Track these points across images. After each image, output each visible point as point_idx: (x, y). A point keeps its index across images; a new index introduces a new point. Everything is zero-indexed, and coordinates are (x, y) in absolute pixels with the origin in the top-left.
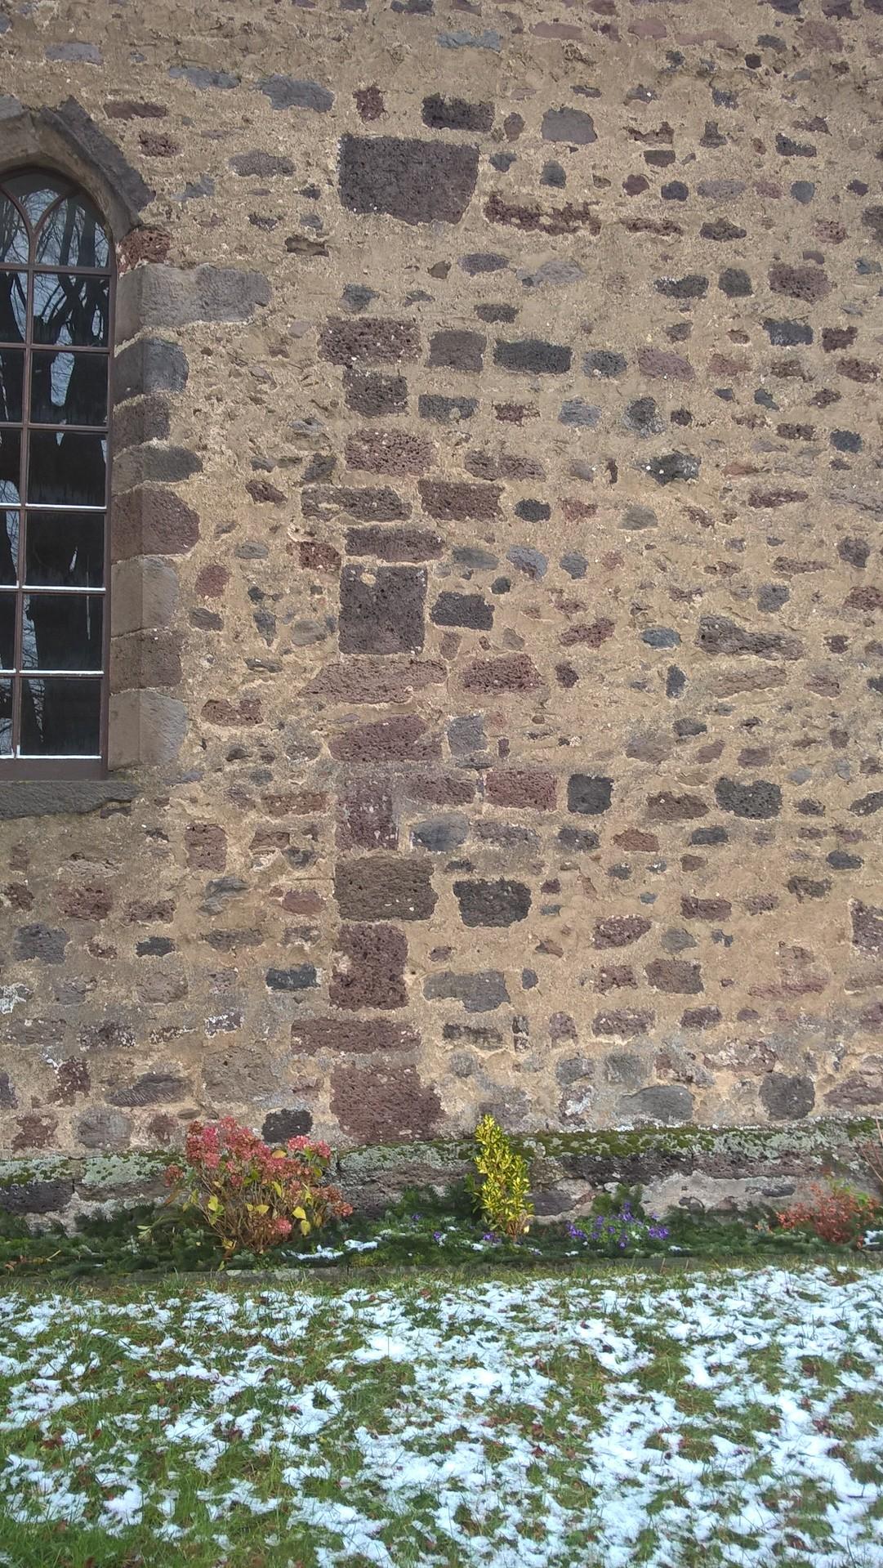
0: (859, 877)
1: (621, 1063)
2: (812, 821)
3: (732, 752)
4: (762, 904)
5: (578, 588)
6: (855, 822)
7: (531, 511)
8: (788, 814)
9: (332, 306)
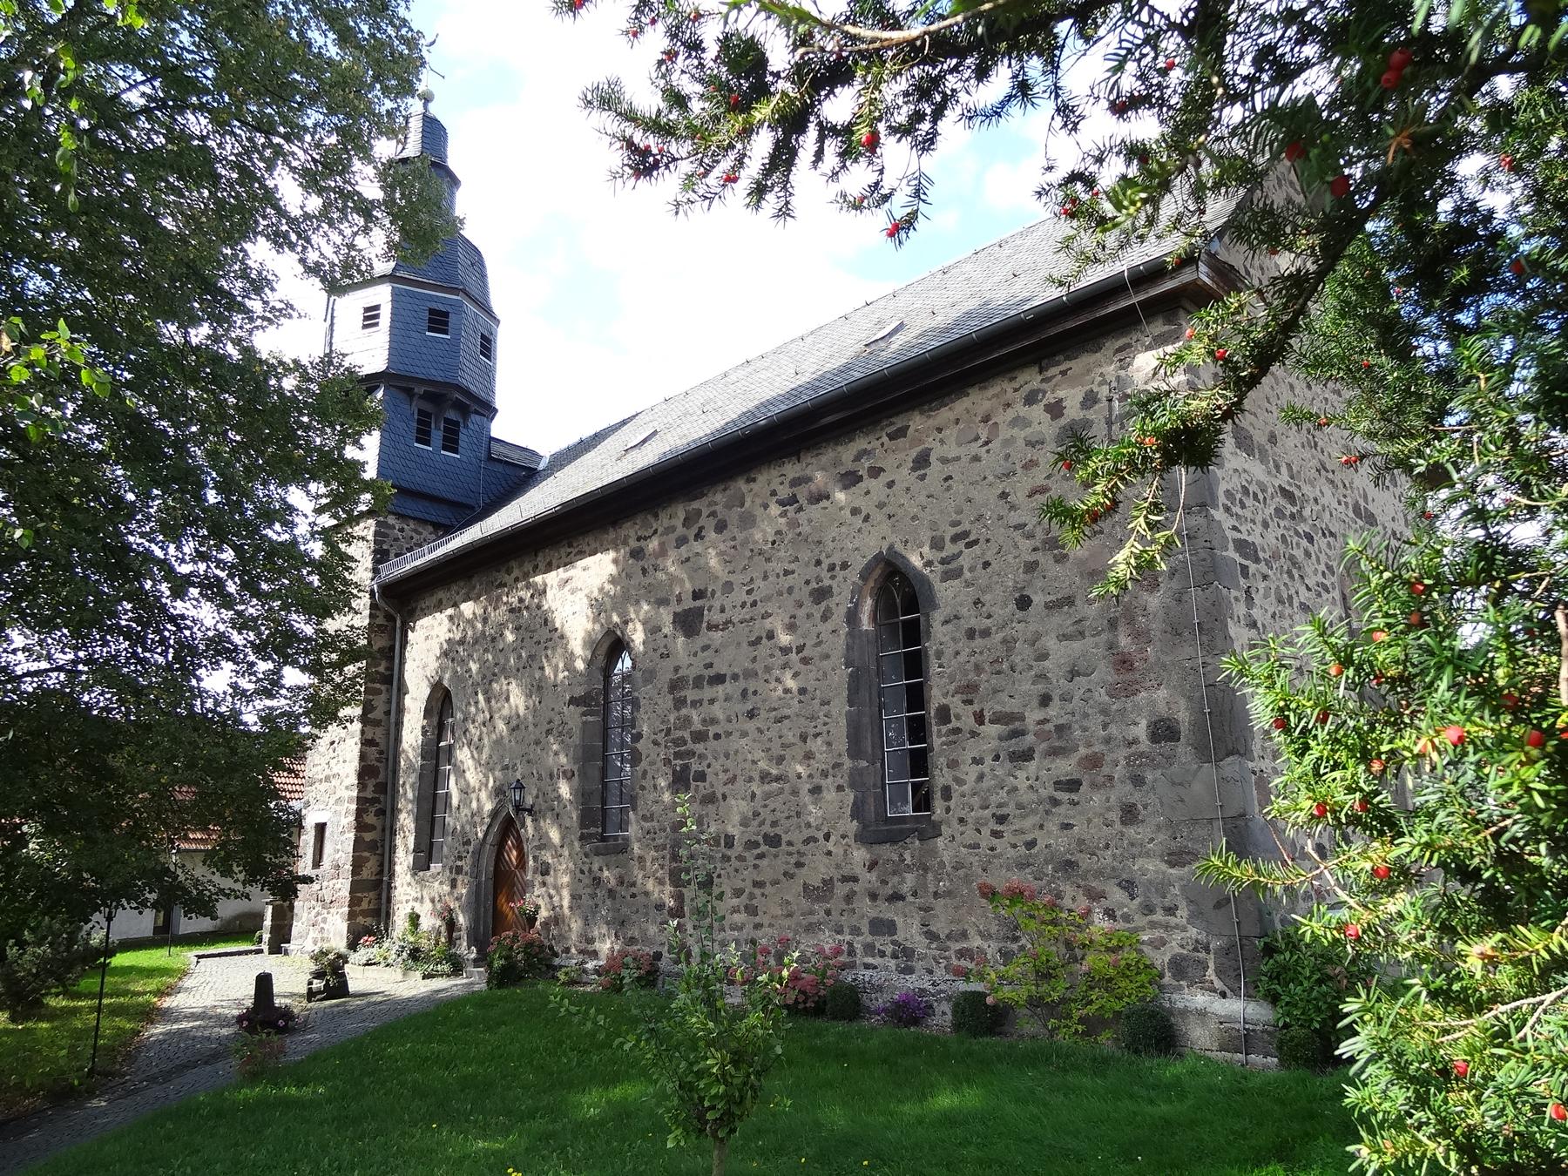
0: (804, 871)
3: (768, 822)
4: (775, 883)
5: (729, 764)
6: (803, 848)
7: (717, 736)
8: (784, 846)
9: (670, 675)
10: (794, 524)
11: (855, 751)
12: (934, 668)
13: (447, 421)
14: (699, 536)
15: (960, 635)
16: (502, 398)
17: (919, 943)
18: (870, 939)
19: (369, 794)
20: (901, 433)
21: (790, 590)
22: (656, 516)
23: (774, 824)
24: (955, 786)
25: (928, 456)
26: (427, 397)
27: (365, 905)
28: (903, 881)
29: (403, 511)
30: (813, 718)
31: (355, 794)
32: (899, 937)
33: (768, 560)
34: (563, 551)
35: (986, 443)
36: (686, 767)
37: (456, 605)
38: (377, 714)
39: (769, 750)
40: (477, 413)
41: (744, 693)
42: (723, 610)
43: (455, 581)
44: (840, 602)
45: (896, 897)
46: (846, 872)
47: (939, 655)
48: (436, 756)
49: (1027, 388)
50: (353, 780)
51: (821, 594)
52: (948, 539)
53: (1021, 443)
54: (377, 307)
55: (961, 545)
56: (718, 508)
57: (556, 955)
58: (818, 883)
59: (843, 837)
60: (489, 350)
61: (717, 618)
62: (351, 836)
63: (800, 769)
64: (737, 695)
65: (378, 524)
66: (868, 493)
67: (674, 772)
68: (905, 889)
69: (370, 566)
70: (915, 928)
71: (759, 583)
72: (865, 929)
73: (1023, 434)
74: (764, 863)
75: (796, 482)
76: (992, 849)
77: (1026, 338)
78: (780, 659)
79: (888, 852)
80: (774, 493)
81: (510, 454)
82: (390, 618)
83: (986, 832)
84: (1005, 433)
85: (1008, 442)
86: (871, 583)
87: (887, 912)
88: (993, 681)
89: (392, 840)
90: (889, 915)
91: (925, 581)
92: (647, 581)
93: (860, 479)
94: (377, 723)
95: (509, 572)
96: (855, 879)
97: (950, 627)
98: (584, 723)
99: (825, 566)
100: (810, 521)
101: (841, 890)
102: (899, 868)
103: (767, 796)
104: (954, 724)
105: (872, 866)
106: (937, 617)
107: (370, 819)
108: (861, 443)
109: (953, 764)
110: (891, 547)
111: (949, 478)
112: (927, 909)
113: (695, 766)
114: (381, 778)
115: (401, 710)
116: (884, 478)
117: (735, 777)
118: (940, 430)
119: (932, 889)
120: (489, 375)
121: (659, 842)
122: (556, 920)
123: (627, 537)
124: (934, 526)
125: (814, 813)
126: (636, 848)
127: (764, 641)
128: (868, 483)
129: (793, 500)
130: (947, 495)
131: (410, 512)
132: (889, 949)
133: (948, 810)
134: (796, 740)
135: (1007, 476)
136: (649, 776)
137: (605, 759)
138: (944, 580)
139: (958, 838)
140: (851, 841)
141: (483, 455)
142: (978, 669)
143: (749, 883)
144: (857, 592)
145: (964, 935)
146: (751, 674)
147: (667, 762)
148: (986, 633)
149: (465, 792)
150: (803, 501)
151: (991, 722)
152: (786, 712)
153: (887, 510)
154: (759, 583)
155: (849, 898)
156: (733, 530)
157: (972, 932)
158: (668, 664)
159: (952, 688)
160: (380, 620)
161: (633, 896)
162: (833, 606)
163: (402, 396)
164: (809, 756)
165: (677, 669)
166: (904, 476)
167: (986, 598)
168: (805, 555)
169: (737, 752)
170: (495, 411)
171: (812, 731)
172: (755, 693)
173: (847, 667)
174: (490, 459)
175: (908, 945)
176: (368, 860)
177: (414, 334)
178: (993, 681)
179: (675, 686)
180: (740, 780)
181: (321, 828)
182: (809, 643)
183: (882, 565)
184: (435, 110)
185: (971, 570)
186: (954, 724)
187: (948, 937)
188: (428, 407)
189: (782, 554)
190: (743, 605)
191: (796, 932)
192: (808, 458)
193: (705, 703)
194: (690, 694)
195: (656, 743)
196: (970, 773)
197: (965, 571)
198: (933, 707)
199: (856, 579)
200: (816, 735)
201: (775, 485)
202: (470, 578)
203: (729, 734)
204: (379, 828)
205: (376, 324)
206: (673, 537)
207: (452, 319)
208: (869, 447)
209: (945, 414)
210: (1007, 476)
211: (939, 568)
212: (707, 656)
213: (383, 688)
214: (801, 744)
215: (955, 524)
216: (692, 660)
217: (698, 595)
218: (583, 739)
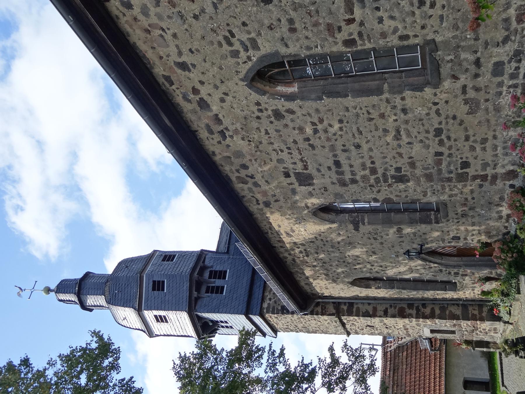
0: (458, 115)
1: (504, 148)
2: (444, 123)
3: (427, 135)
4: (466, 129)
5: (390, 156)
6: (443, 116)
7: (373, 163)
8: (443, 126)
10: (236, 131)
11: (379, 91)
12: (319, 50)
13: (210, 277)
14: (252, 177)
15: (294, 36)
16: (196, 247)
17: (510, 47)
18: (506, 76)
19: (414, 312)
20: (168, 79)
21: (277, 131)
22: (243, 197)
23: (427, 132)
24: (399, 33)
25: (179, 63)
26: (198, 290)
27: (476, 312)
28: (466, 60)
29: (260, 299)
30: (358, 115)
31: (414, 320)
32: (505, 59)
33: (261, 143)
34: (270, 235)
35: (163, 30)
36: (393, 177)
37: (307, 278)
38: (370, 309)
39: (379, 137)
40: (204, 262)
41: (344, 151)
42: (295, 163)
43: (295, 279)
44: (282, 105)
45: (477, 63)
46: (459, 92)
47: (308, 48)
49: (121, 8)
50: (407, 321)
51: (278, 115)
52: (230, 48)
53: (158, 10)
54: (156, 316)
55: (233, 40)
56: (233, 169)
57: (509, 233)
58: (467, 107)
59: (435, 95)
60: (170, 256)
61: (299, 167)
62: (437, 321)
63: (391, 120)
64: (346, 154)
65: (268, 312)
66: (209, 95)
67: (395, 182)
68: (471, 58)
69: (290, 316)
70: (500, 50)
71: (276, 146)
72: (499, 79)
73: (152, 9)
74: (453, 136)
75: (211, 132)
76: (443, 7)
77: (87, 17)
78: (321, 134)
79: (446, 69)
80: (219, 142)
81: (224, 240)
82: (318, 304)
83: (431, 12)
84: (154, 20)
85: (160, 17)
86: (267, 88)
87: (488, 66)
88: (324, 15)
89: (439, 300)
90: (490, 66)
91: (261, 59)
92: (281, 198)
93: (201, 99)
94: (375, 309)
95: (287, 258)
96: (464, 87)
97: (289, 43)
98: (369, 223)
99: (260, 114)
100: (233, 124)
101: (471, 94)
102: (457, 62)
103: (409, 135)
104: (355, 36)
105: (455, 78)
106: (283, 51)
107: (428, 311)
108: (179, 99)
109: (384, 35)
110: (242, 80)
111: (191, 50)
112: (486, 44)
113: (393, 172)
114: (405, 306)
115: (367, 298)
116: (198, 86)
117: (398, 153)
118: (161, 58)
119: (473, 42)
120: (184, 255)
121: (439, 188)
122: (488, 233)
123: (258, 209)
124: (224, 57)
125: (420, 111)
126: (444, 198)
127: (310, 142)
128: (203, 93)
129: (222, 133)
130: (202, 51)
131: (261, 296)
132: (514, 65)
133: (416, 36)
134: (372, 123)
135: (182, 17)
136: (399, 194)
137: (390, 211)
138: (258, 49)
139: (436, 28)
140: (438, 91)
141: (226, 256)
142: (316, 24)
143: (466, 143)
144: (274, 95)
145: (507, 20)
146: (333, 148)
147: (390, 186)
148: (291, 21)
149: (411, 270)
150: (221, 128)
151: (352, 13)
152: (354, 129)
153: (218, 83)
154: (276, 146)
155: (477, 89)
156: (245, 161)
157: (504, 16)
158: (331, 188)
159: (331, 39)
160: (319, 309)
161: (473, 198)
162: (284, 109)
163: (199, 303)
164: (382, 116)
165: (333, 183)
166: (195, 75)
167: (267, 22)
168: (255, 124)
169: (382, 153)
170: (202, 251)
171: (366, 115)
172: (344, 146)
173: (323, 99)
174: (228, 252)
175: (512, 53)
176: (451, 311)
178: (324, 15)
179: (343, 184)
180: (399, 150)
181: (432, 331)
182: (309, 119)
183: (254, 83)
185: (249, 33)
186: (355, 36)
187: (507, 29)
188: (204, 289)
189: (256, 136)
190: (291, 154)
191: (500, 117)
192: (195, 127)
193: (353, 169)
194: (348, 176)
195: (379, 191)
196: (389, 24)
197: (250, 36)
198: (344, 49)
199: (265, 98)
200: (369, 113)
201: (215, 142)
202: (291, 273)
203: (371, 157)
204: (433, 306)
205: (165, 317)
206: (254, 189)
207: (156, 279)
208: (181, 96)
209: (150, 55)
210: (182, 17)
211: (251, 52)
212: (324, 170)
213: (355, 306)
214: (374, 121)
215: (220, 44)
216: (327, 176)
217: (287, 175)
218: (378, 224)
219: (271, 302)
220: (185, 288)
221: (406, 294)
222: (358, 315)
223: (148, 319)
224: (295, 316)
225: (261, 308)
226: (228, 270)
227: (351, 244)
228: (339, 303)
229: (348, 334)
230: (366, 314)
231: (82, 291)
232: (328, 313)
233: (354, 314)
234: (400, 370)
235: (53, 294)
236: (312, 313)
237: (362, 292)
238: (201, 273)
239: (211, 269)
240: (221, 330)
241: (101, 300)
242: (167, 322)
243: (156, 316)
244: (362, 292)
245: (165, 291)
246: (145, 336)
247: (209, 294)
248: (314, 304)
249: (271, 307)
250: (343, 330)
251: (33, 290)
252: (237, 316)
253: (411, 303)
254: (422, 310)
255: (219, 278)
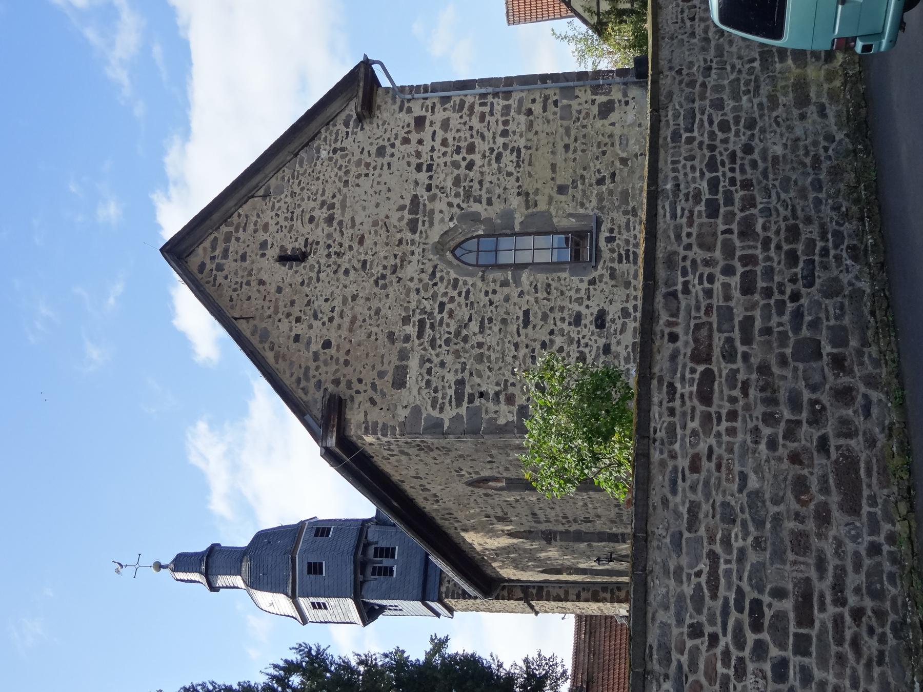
13: (375, 556)
19: (608, 596)
26: (363, 573)
38: (562, 593)
40: (366, 537)
48: (584, 572)
50: (601, 604)
54: (313, 604)
65: (447, 597)
94: (567, 593)
98: (561, 540)
115: (558, 582)
160: (505, 593)
163: (366, 586)
177: (326, 583)
184: (167, 560)
194: (543, 518)
205: (324, 604)
213: (545, 590)
219: (450, 585)
220: (348, 570)
221: (599, 579)
222: (548, 600)
223: (303, 606)
224: (478, 601)
225: (440, 593)
226: (397, 547)
227: (542, 550)
228: (528, 587)
229: (537, 613)
230: (558, 599)
231: (209, 571)
232: (515, 597)
233: (544, 598)
234: (598, 634)
235: (166, 572)
236: (497, 598)
237: (554, 577)
238: (364, 553)
239: (376, 546)
240: (387, 612)
241: (238, 581)
242: (326, 608)
243: (313, 604)
244: (554, 577)
245: (324, 575)
246: (297, 625)
247: (376, 577)
248: (500, 588)
249: (451, 592)
250: (530, 611)
251: (137, 566)
252: (411, 602)
253: (605, 587)
254: (617, 593)
255: (387, 557)
